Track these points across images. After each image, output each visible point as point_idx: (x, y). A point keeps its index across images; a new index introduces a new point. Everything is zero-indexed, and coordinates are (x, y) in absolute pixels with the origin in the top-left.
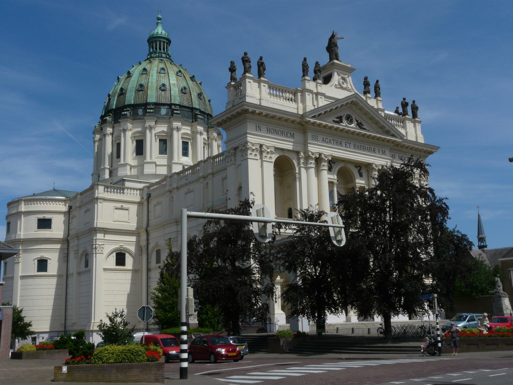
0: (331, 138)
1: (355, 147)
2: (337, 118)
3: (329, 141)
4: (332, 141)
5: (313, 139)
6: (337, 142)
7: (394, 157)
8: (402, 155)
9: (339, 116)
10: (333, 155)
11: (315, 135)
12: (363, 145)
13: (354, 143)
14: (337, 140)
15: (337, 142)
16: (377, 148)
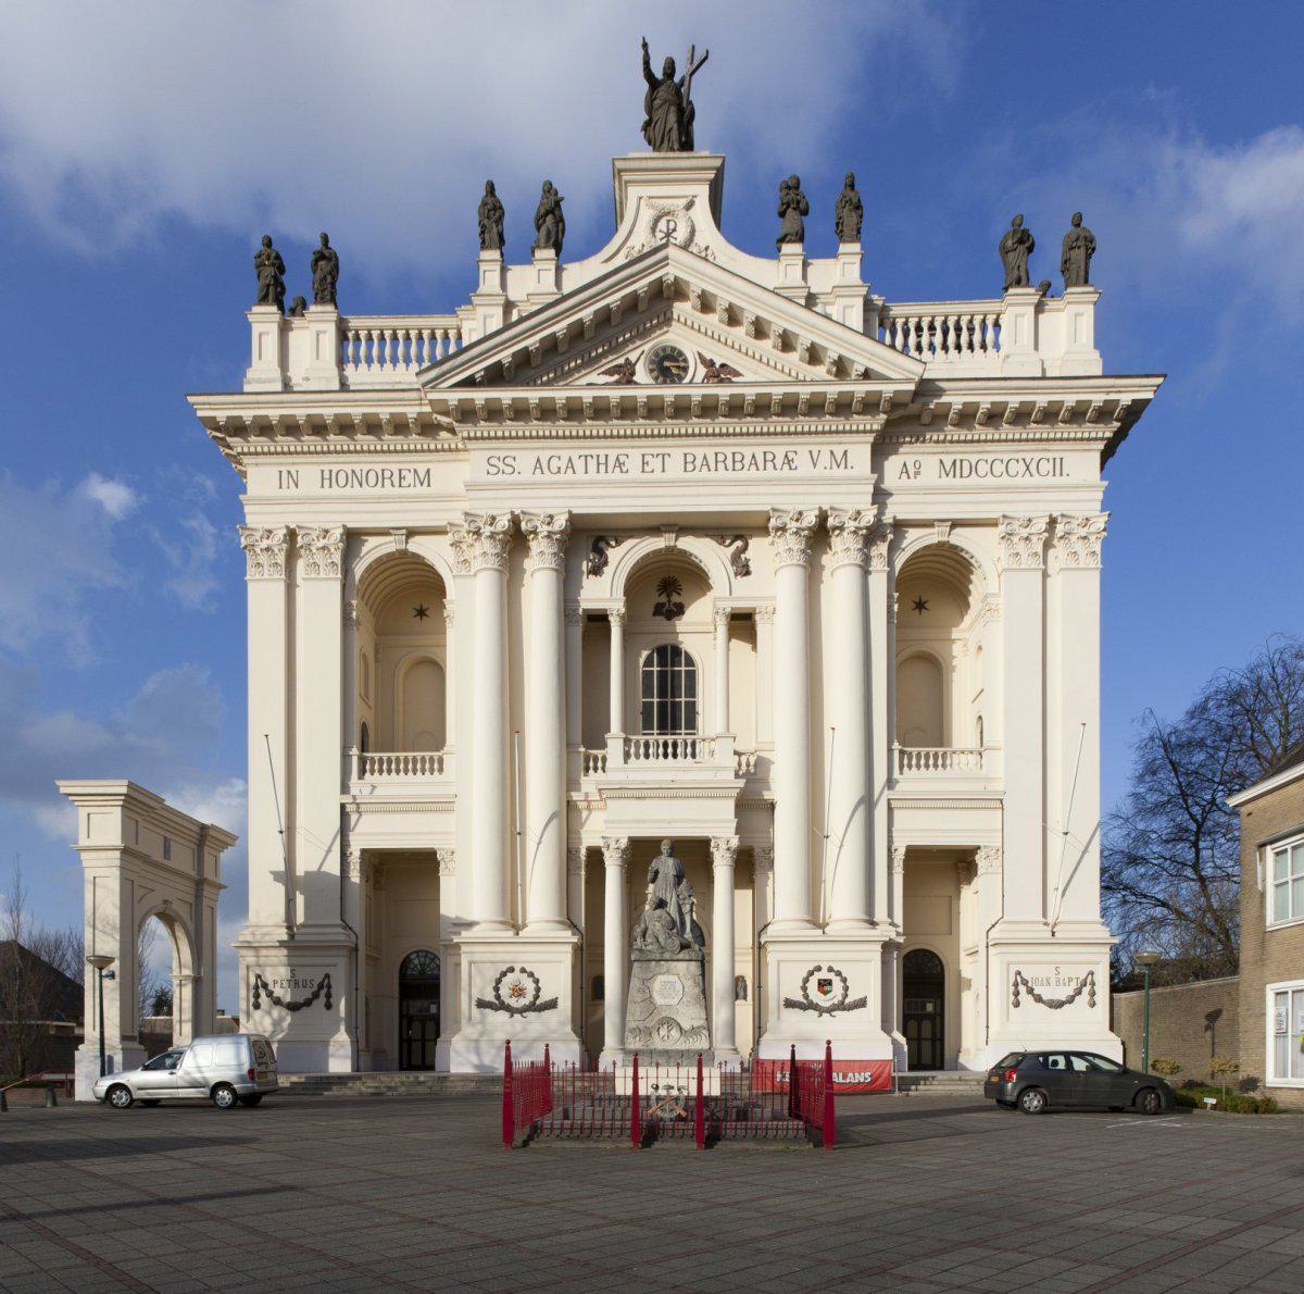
0: (575, 454)
1: (690, 467)
2: (609, 372)
3: (563, 464)
4: (579, 464)
5: (495, 470)
6: (602, 460)
7: (911, 470)
8: (958, 457)
9: (621, 361)
10: (575, 511)
11: (502, 454)
12: (728, 451)
13: (686, 450)
14: (602, 453)
15: (602, 460)
16: (803, 451)
